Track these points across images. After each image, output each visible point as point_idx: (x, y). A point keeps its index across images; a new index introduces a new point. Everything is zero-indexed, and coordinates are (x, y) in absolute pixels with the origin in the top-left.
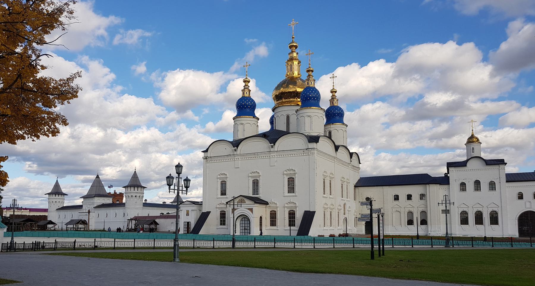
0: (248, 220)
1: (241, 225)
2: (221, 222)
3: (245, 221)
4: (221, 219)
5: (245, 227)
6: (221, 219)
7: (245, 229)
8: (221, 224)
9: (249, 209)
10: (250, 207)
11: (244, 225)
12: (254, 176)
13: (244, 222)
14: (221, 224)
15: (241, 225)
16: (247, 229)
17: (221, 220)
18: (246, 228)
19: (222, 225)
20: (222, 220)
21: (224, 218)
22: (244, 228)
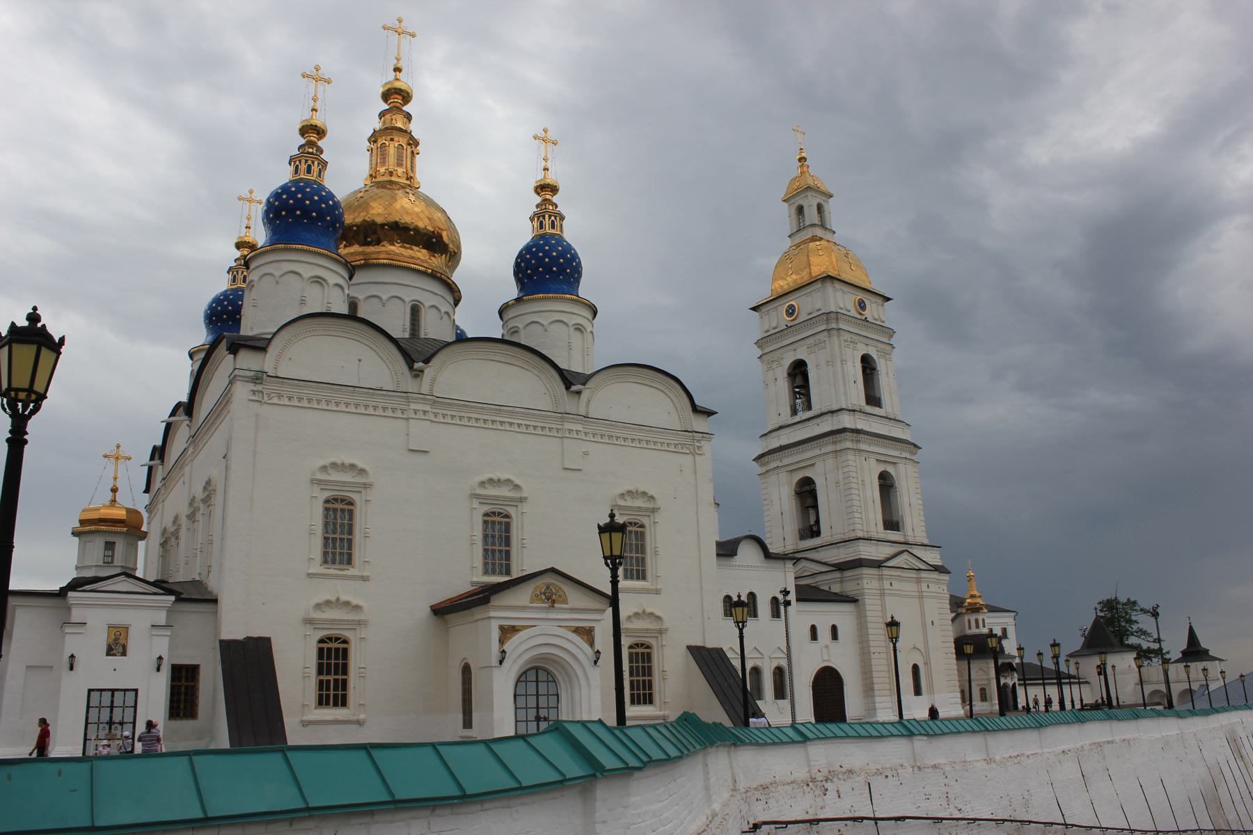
0: (550, 679)
1: (521, 700)
2: (321, 689)
3: (537, 681)
4: (324, 678)
5: (538, 708)
6: (324, 678)
7: (538, 719)
8: (322, 701)
9: (577, 630)
10: (584, 620)
11: (532, 702)
12: (496, 498)
13: (532, 688)
14: (322, 701)
15: (521, 700)
16: (546, 719)
17: (321, 682)
18: (543, 713)
19: (328, 704)
20: (328, 681)
21: (336, 673)
22: (532, 714)
